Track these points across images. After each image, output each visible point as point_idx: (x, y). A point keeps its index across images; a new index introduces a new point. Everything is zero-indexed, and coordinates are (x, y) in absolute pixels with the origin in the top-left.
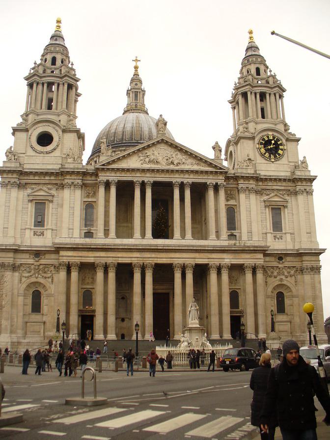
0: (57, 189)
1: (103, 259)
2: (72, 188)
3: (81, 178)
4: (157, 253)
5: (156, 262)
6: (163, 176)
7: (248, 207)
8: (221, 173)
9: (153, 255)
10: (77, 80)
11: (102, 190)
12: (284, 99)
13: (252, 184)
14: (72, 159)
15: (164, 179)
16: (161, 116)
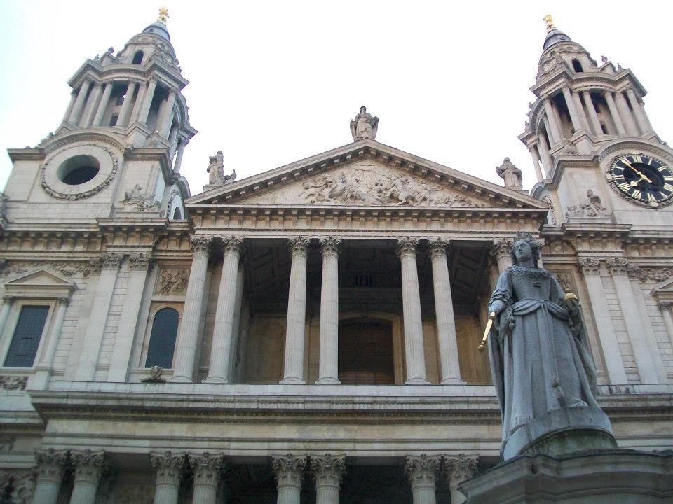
0: (85, 275)
1: (181, 444)
2: (125, 267)
3: (150, 244)
4: (355, 427)
5: (349, 454)
6: (370, 226)
7: (616, 308)
8: (528, 216)
9: (341, 432)
10: (182, 84)
11: (199, 264)
12: (646, 108)
13: (613, 251)
14: (135, 206)
15: (373, 234)
16: (363, 108)
